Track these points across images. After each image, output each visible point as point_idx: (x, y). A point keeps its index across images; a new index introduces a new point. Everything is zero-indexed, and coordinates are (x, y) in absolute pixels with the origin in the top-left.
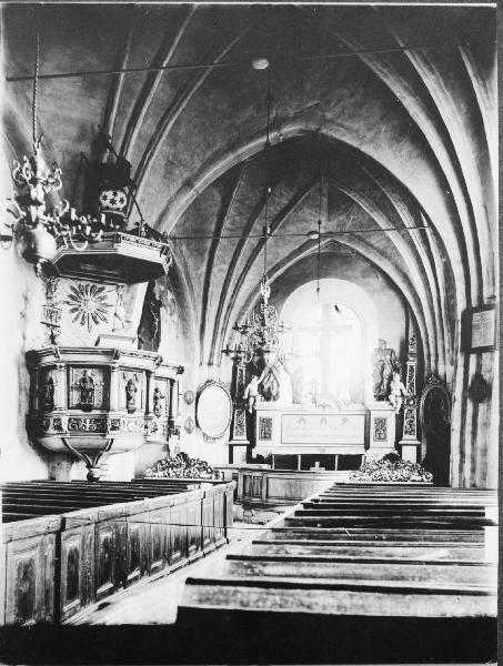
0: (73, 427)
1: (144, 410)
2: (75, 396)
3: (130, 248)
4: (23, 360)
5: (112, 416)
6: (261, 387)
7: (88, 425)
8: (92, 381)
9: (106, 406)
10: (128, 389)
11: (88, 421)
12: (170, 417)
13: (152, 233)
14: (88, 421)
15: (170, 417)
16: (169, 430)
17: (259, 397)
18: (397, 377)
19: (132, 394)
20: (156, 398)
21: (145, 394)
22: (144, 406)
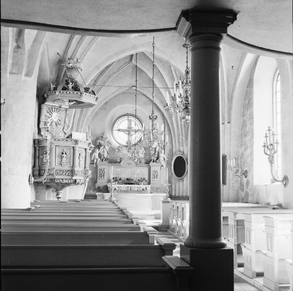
2: (58, 160)
5: (76, 169)
6: (100, 154)
8: (66, 154)
17: (99, 160)
18: (163, 151)
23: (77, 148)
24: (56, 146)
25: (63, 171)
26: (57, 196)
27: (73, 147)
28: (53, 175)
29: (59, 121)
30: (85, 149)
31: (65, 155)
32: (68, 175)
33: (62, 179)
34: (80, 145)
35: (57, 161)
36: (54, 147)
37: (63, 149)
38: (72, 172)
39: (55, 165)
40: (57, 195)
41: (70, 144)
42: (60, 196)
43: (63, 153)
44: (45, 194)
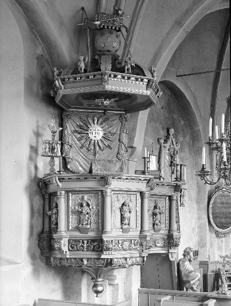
0: (72, 248)
1: (139, 229)
2: (73, 220)
3: (117, 84)
4: (35, 188)
5: (105, 238)
7: (85, 245)
8: (88, 205)
9: (101, 228)
10: (121, 209)
11: (85, 242)
12: (170, 230)
13: (138, 70)
14: (85, 242)
15: (170, 230)
16: (169, 243)
19: (127, 215)
20: (154, 214)
21: (139, 214)
22: (139, 225)
23: (109, 191)
24: (67, 192)
25: (83, 243)
26: (95, 289)
27: (102, 191)
28: (60, 249)
29: (103, 139)
30: (142, 194)
31: (86, 209)
32: (93, 250)
33: (82, 260)
34: (114, 184)
35: (71, 220)
36: (63, 192)
37: (83, 198)
38: (98, 245)
39: (68, 230)
40: (95, 286)
41: (91, 184)
42: (100, 289)
43: (82, 206)
44: (81, 280)
